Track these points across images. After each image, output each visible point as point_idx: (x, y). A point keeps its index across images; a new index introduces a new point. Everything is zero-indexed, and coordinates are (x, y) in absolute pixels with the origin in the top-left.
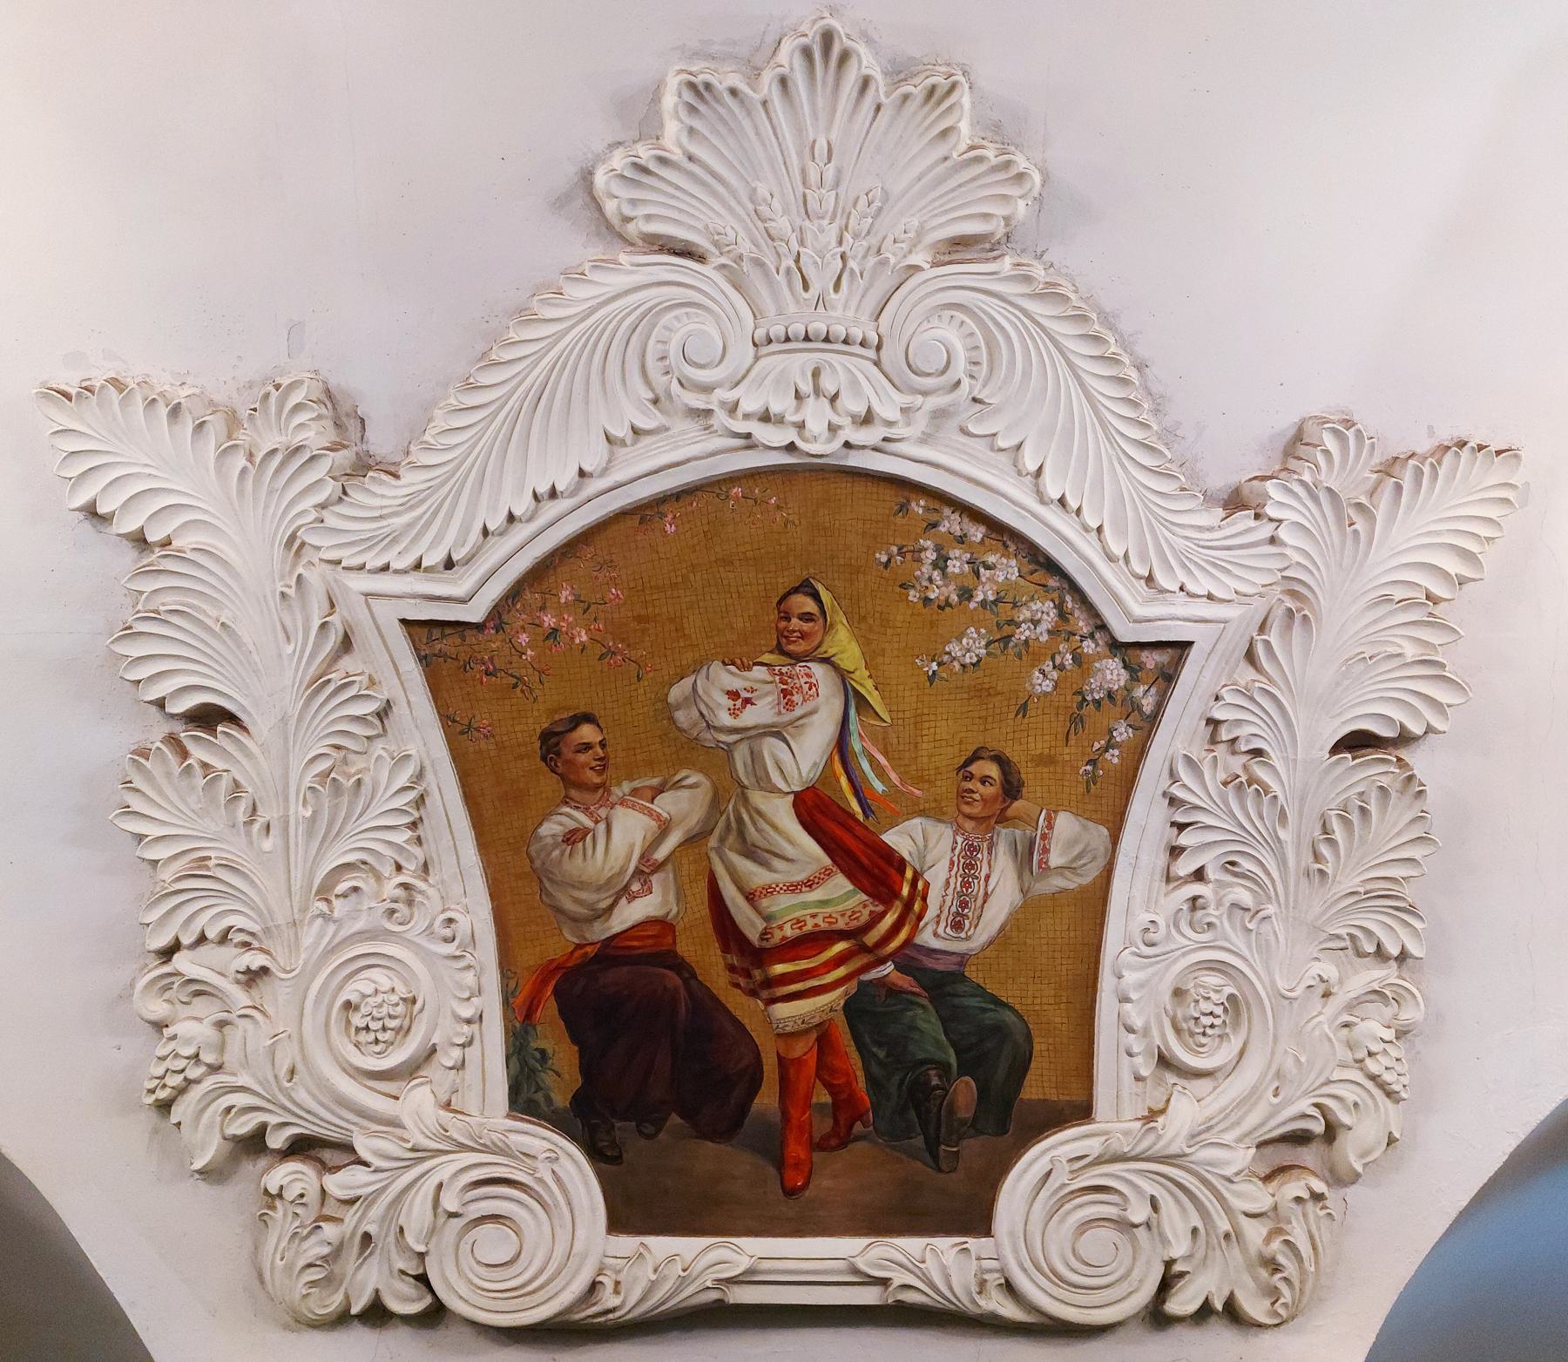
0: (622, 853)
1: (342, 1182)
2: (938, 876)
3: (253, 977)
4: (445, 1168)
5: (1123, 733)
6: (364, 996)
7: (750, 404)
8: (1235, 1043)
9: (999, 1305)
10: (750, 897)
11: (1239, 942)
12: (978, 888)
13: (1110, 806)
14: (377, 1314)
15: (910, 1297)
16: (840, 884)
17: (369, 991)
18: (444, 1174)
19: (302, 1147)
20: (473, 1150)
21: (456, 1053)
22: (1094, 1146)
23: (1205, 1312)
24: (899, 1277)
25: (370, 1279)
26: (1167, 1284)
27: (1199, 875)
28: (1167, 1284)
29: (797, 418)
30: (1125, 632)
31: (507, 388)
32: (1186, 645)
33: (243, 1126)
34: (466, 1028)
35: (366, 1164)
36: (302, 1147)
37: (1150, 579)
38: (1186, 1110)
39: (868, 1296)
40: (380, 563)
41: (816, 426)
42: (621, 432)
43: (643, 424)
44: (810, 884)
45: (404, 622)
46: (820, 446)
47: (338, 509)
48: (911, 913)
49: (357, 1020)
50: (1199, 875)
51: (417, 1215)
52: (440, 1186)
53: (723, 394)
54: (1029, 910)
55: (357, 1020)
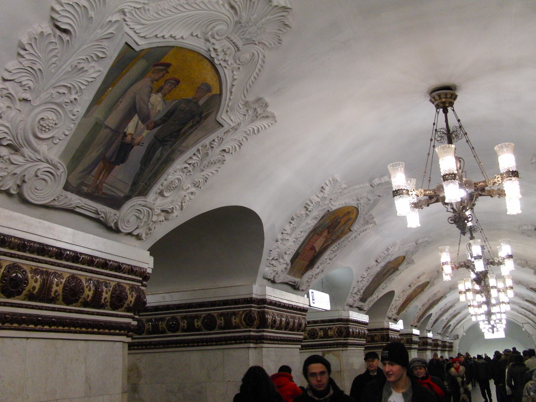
1: (17, 158)
4: (44, 166)
6: (48, 119)
7: (216, 47)
15: (101, 219)
17: (50, 118)
18: (41, 167)
20: (49, 164)
21: (58, 141)
24: (103, 215)
29: (218, 53)
31: (186, 10)
32: (223, 126)
34: (64, 136)
35: (24, 157)
37: (227, 111)
40: (133, 27)
41: (220, 57)
42: (195, 34)
43: (199, 36)
45: (126, 43)
46: (216, 62)
47: (137, 11)
49: (42, 122)
52: (39, 169)
53: (215, 42)
55: (42, 122)
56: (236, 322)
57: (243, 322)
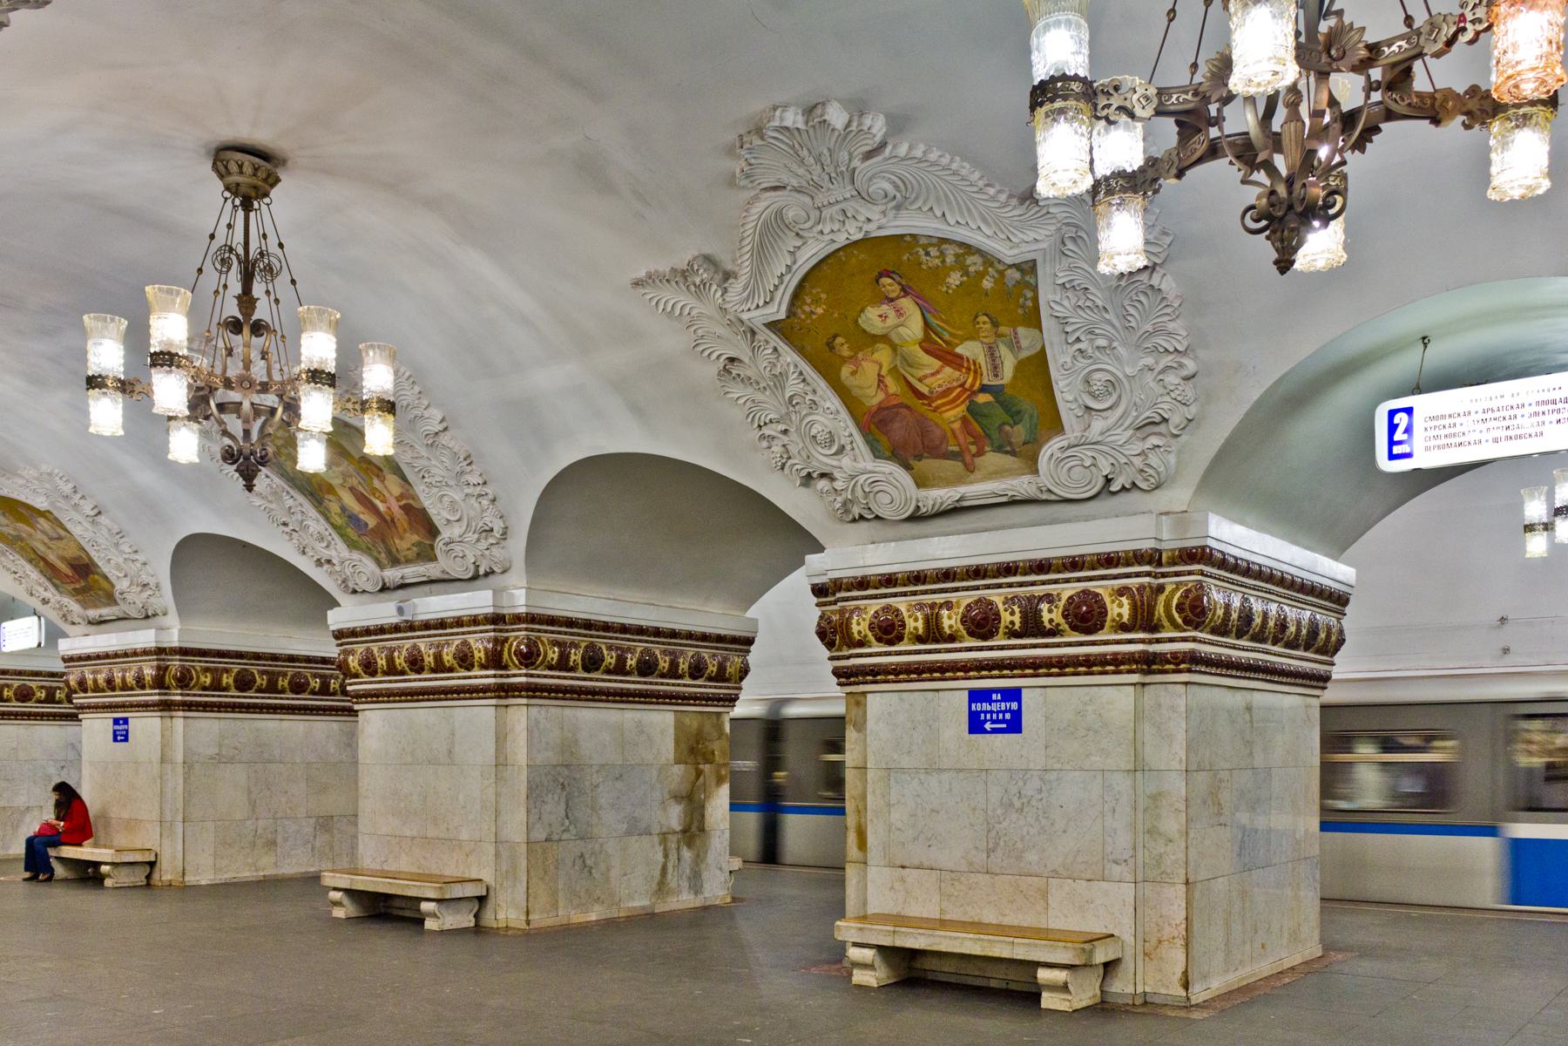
0: (869, 376)
2: (981, 360)
3: (785, 432)
5: (1029, 294)
8: (1115, 397)
9: (1045, 496)
10: (920, 380)
11: (1107, 359)
12: (998, 362)
13: (1033, 318)
14: (862, 517)
16: (948, 370)
19: (823, 475)
22: (1065, 443)
23: (1124, 489)
25: (856, 511)
26: (1108, 481)
27: (1078, 340)
28: (1108, 481)
30: (1009, 261)
33: (804, 473)
36: (823, 475)
38: (1098, 425)
39: (1004, 499)
44: (938, 372)
48: (977, 372)
50: (1078, 340)
51: (859, 493)
54: (1020, 366)
56: (1051, 621)
57: (1176, 615)
